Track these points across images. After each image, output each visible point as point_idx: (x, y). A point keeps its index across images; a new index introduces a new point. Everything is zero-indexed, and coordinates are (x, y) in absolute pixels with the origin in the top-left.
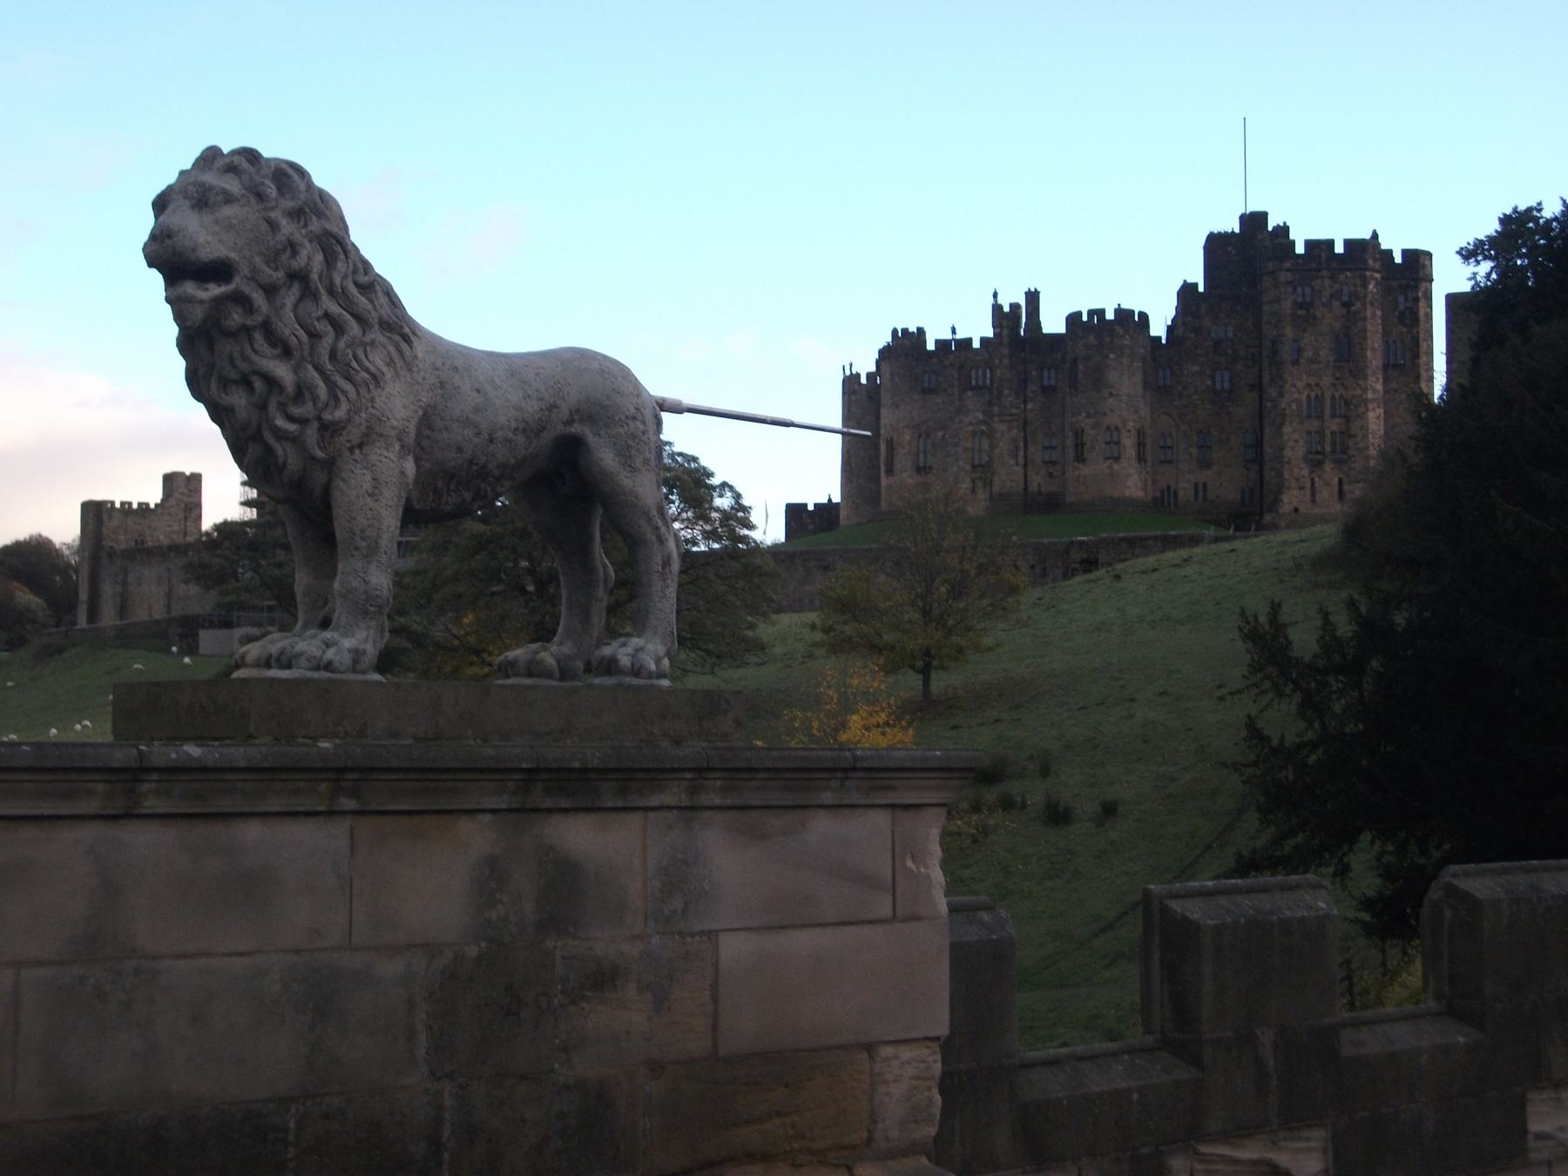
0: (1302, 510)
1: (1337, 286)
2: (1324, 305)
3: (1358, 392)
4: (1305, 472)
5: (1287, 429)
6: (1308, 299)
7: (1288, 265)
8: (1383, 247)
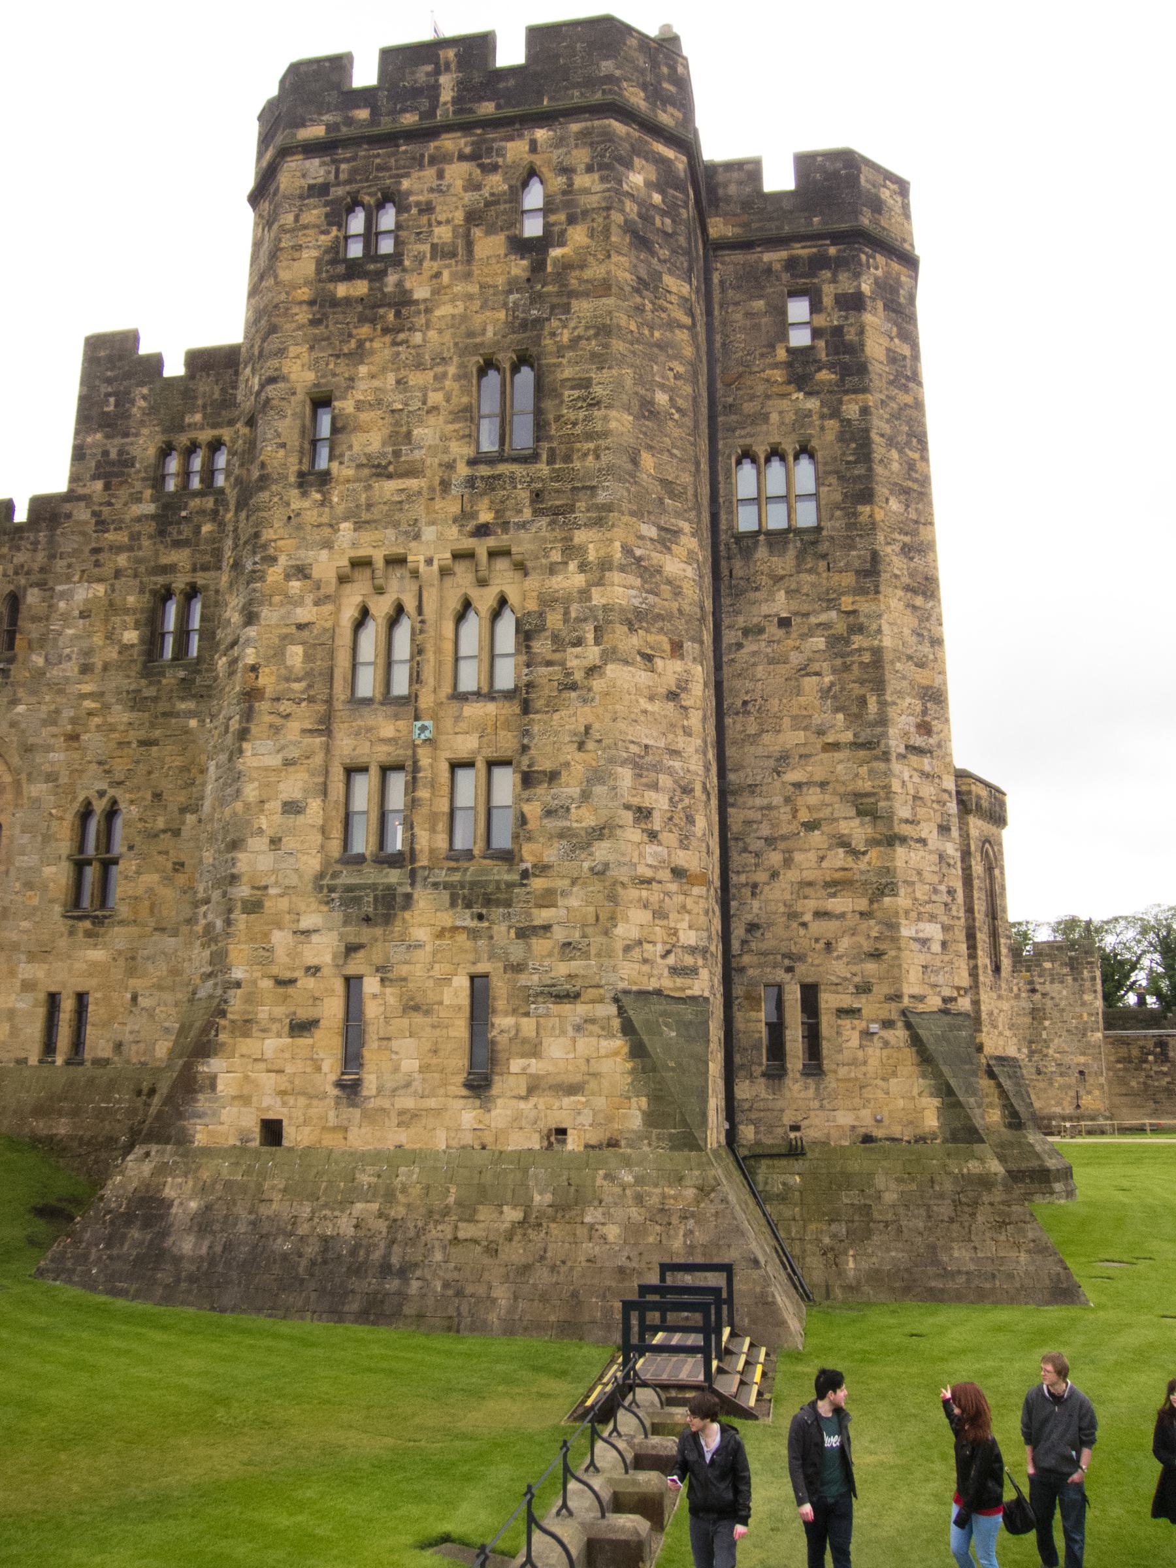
0: (291, 1136)
1: (496, 183)
2: (437, 252)
3: (572, 579)
4: (323, 949)
5: (259, 755)
6: (386, 246)
7: (315, 131)
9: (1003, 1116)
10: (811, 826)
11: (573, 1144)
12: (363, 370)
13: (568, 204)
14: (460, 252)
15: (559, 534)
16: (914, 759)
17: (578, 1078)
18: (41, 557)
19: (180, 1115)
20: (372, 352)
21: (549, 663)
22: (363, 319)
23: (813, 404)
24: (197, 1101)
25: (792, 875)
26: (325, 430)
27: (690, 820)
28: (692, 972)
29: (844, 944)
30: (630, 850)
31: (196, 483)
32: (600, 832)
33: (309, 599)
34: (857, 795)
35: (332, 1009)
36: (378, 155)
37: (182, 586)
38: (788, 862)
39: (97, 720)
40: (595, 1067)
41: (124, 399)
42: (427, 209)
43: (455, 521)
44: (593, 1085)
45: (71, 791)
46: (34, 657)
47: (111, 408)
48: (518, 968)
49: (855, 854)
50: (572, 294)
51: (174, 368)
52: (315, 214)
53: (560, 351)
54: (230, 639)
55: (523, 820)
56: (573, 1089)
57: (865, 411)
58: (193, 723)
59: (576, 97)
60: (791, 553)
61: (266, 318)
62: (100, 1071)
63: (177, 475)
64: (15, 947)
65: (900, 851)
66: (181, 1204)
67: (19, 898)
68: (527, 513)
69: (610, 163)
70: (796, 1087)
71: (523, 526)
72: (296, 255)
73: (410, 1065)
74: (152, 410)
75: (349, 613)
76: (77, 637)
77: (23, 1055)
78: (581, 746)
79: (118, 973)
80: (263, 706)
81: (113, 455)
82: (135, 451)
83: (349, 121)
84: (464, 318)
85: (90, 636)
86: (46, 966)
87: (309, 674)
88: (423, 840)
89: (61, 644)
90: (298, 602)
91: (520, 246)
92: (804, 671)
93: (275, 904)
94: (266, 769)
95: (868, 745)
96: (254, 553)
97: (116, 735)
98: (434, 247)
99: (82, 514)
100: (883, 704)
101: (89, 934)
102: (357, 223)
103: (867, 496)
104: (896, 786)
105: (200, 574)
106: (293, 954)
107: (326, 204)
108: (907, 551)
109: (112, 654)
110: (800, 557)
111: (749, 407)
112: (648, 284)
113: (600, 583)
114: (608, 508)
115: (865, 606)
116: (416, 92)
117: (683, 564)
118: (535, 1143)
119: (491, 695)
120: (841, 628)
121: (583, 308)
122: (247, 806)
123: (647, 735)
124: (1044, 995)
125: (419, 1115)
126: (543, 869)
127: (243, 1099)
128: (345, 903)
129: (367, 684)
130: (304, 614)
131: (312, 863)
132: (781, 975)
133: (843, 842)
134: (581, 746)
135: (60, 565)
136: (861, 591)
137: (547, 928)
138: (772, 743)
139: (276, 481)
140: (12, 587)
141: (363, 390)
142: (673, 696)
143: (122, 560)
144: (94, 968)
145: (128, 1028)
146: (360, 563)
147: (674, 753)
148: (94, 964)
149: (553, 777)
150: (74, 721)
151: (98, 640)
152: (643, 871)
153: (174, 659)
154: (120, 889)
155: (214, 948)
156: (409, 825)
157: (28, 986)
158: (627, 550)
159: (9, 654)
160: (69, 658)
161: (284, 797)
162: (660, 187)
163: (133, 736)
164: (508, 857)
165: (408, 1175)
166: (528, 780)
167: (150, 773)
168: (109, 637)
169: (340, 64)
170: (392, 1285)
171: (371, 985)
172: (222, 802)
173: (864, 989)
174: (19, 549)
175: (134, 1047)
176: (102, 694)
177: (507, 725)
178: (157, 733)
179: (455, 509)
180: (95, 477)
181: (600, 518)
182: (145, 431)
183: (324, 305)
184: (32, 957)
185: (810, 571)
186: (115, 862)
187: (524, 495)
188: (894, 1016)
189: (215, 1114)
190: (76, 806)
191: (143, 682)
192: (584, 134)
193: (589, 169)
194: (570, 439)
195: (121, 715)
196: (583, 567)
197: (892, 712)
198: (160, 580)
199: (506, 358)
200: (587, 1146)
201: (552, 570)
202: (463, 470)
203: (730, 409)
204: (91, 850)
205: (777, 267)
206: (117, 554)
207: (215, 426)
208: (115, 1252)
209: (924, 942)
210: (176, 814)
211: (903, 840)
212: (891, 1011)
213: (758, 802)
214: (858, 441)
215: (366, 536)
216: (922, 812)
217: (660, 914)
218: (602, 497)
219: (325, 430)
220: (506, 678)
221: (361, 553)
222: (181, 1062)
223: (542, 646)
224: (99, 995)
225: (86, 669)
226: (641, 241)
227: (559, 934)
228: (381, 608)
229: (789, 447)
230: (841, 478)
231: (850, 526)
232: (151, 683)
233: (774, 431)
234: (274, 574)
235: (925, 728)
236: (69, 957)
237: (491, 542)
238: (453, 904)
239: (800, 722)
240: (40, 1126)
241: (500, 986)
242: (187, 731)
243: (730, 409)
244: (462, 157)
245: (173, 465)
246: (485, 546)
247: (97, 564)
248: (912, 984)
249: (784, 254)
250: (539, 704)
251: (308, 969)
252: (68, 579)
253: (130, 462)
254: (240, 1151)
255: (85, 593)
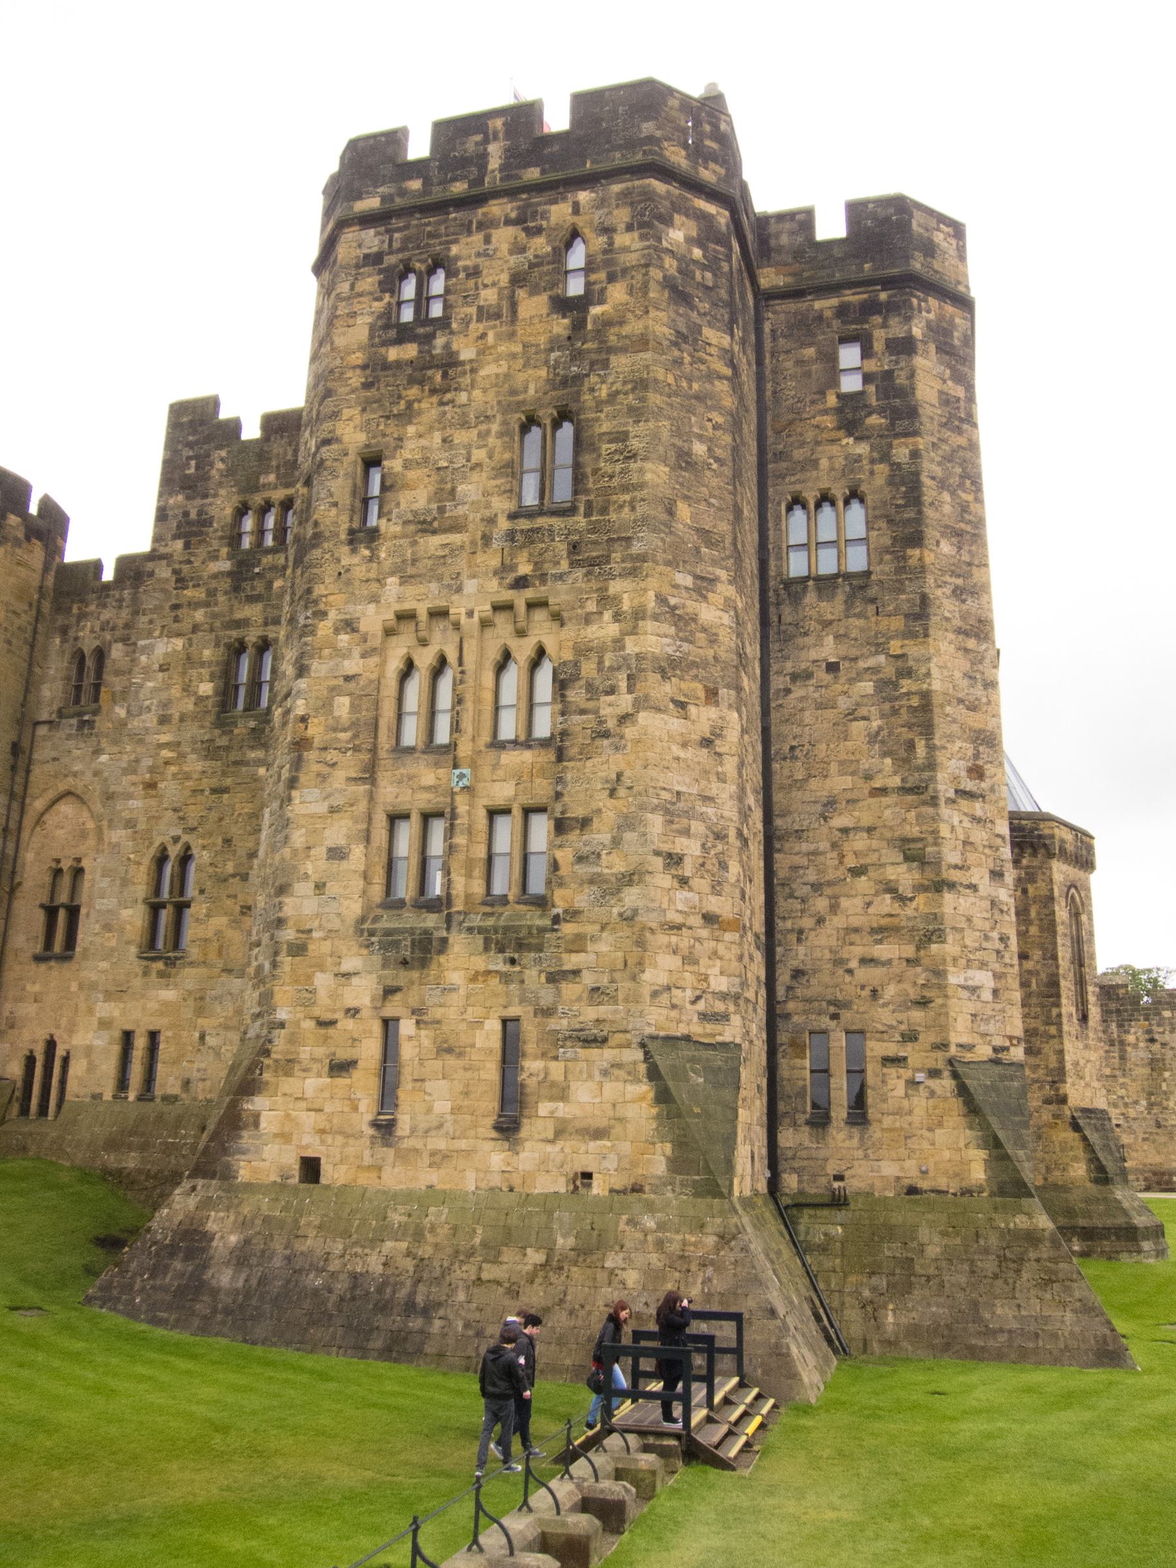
0: (328, 1173)
1: (540, 245)
2: (484, 314)
3: (606, 629)
5: (307, 802)
7: (371, 203)
8: (766, 198)
9: (1089, 1170)
10: (857, 872)
11: (598, 1188)
12: (411, 430)
13: (608, 263)
14: (506, 313)
15: (594, 585)
16: (964, 804)
17: (602, 1123)
18: (125, 614)
19: (225, 1151)
20: (420, 413)
21: (583, 712)
22: (412, 381)
23: (863, 449)
24: (240, 1137)
25: (838, 921)
26: (375, 490)
27: (723, 866)
28: (724, 1017)
29: (890, 992)
30: (660, 896)
31: (269, 541)
32: (629, 878)
33: (356, 652)
34: (905, 840)
35: (370, 1050)
36: (429, 224)
37: (254, 640)
38: (834, 908)
39: (173, 769)
40: (621, 1111)
41: (203, 461)
42: (475, 272)
43: (495, 573)
44: (617, 1130)
45: (147, 836)
46: (117, 709)
47: (192, 471)
48: (547, 1012)
49: (902, 900)
50: (611, 350)
51: (251, 431)
52: (369, 282)
53: (599, 405)
54: (285, 690)
55: (555, 866)
56: (599, 1134)
57: (915, 454)
58: (262, 771)
59: (618, 159)
60: (840, 597)
61: (324, 385)
62: (167, 1108)
63: (252, 533)
64: (93, 986)
65: (948, 897)
66: (222, 1237)
67: (98, 940)
68: (564, 565)
69: (649, 220)
70: (840, 1136)
71: (560, 577)
72: (351, 322)
73: (442, 1106)
74: (230, 472)
75: (395, 665)
76: (156, 689)
77: (98, 1091)
78: (612, 793)
79: (187, 1013)
80: (311, 756)
81: (193, 515)
82: (213, 511)
83: (403, 193)
84: (507, 376)
85: (168, 687)
86: (122, 1005)
87: (354, 724)
88: (459, 884)
89: (142, 696)
90: (347, 655)
91: (562, 305)
92: (852, 715)
93: (319, 947)
94: (312, 816)
95: (916, 790)
96: (306, 608)
97: (190, 783)
98: (480, 309)
99: (164, 572)
100: (931, 748)
101: (161, 974)
102: (409, 290)
103: (916, 539)
104: (945, 831)
105: (270, 627)
106: (334, 996)
107: (380, 272)
108: (959, 593)
109: (189, 706)
110: (849, 602)
111: (798, 454)
112: (687, 338)
113: (634, 631)
114: (643, 558)
115: (913, 650)
116: (465, 162)
117: (723, 612)
118: (561, 1187)
119: (526, 742)
120: (889, 672)
121: (621, 363)
122: (295, 852)
123: (679, 781)
124: (1164, 1045)
125: (451, 1157)
126: (573, 914)
127: (284, 1137)
128: (384, 947)
129: (411, 734)
130: (352, 666)
131: (355, 908)
132: (825, 1022)
133: (891, 889)
134: (612, 793)
135: (143, 620)
136: (909, 634)
137: (576, 973)
138: (819, 788)
139: (327, 539)
140: (97, 643)
141: (410, 450)
142: (707, 743)
143: (199, 615)
144: (166, 1008)
145: (196, 1066)
146: (405, 617)
147: (707, 799)
148: (166, 1004)
149: (584, 823)
150: (152, 770)
151: (176, 692)
152: (673, 917)
153: (246, 710)
154: (191, 931)
155: (262, 989)
156: (447, 872)
157: (105, 1024)
158: (661, 599)
159: (94, 706)
160: (149, 709)
161: (329, 843)
162: (700, 242)
163: (206, 784)
164: (541, 902)
165: (438, 1215)
166: (560, 827)
167: (221, 819)
168: (186, 689)
169: (394, 139)
170: (416, 1323)
171: (407, 1027)
172: (273, 848)
173: (910, 1037)
174: (105, 606)
175: (200, 1085)
176: (179, 744)
177: (543, 772)
178: (228, 781)
179: (495, 562)
180: (176, 537)
181: (635, 568)
182: (223, 492)
183: (376, 368)
184: (109, 996)
185: (859, 616)
186: (187, 905)
187: (562, 548)
188: (941, 1065)
189: (258, 1151)
190: (152, 851)
191: (217, 732)
192: (625, 194)
193: (629, 228)
194: (606, 492)
195: (195, 764)
196: (617, 617)
197: (940, 757)
198: (234, 634)
199: (547, 414)
200: (611, 1191)
201: (588, 620)
202: (504, 524)
203: (780, 456)
204: (165, 895)
205: (828, 314)
206: (195, 609)
207: (287, 485)
208: (158, 1282)
209: (974, 990)
210: (244, 860)
211: (952, 886)
212: (938, 1060)
213: (805, 847)
214: (908, 485)
215: (411, 590)
216: (972, 857)
217: (690, 959)
218: (637, 548)
219: (375, 490)
220: (543, 727)
221: (407, 606)
222: (227, 1099)
223: (576, 695)
224: (169, 1034)
225: (164, 720)
226: (679, 295)
227: (588, 979)
228: (425, 660)
229: (839, 492)
230: (891, 521)
231: (900, 570)
232: (224, 733)
233: (825, 475)
234: (324, 628)
235: (977, 772)
236: (143, 996)
237: (529, 593)
238: (487, 949)
239: (848, 767)
240: (111, 1160)
241: (530, 1030)
242: (256, 779)
243: (780, 456)
244: (508, 222)
245: (249, 524)
246: (523, 598)
247: (176, 619)
248: (960, 1033)
249: (834, 301)
250: (573, 751)
251: (348, 1010)
252: (149, 634)
253: (208, 522)
254: (281, 1187)
255: (165, 647)
